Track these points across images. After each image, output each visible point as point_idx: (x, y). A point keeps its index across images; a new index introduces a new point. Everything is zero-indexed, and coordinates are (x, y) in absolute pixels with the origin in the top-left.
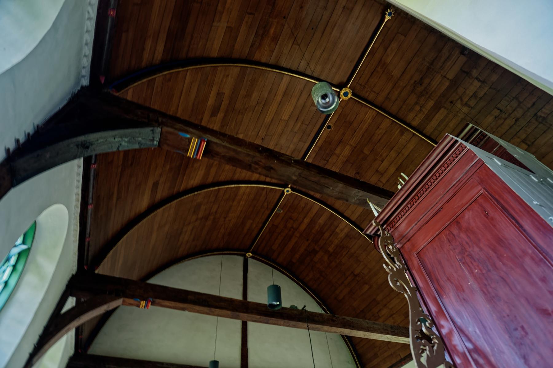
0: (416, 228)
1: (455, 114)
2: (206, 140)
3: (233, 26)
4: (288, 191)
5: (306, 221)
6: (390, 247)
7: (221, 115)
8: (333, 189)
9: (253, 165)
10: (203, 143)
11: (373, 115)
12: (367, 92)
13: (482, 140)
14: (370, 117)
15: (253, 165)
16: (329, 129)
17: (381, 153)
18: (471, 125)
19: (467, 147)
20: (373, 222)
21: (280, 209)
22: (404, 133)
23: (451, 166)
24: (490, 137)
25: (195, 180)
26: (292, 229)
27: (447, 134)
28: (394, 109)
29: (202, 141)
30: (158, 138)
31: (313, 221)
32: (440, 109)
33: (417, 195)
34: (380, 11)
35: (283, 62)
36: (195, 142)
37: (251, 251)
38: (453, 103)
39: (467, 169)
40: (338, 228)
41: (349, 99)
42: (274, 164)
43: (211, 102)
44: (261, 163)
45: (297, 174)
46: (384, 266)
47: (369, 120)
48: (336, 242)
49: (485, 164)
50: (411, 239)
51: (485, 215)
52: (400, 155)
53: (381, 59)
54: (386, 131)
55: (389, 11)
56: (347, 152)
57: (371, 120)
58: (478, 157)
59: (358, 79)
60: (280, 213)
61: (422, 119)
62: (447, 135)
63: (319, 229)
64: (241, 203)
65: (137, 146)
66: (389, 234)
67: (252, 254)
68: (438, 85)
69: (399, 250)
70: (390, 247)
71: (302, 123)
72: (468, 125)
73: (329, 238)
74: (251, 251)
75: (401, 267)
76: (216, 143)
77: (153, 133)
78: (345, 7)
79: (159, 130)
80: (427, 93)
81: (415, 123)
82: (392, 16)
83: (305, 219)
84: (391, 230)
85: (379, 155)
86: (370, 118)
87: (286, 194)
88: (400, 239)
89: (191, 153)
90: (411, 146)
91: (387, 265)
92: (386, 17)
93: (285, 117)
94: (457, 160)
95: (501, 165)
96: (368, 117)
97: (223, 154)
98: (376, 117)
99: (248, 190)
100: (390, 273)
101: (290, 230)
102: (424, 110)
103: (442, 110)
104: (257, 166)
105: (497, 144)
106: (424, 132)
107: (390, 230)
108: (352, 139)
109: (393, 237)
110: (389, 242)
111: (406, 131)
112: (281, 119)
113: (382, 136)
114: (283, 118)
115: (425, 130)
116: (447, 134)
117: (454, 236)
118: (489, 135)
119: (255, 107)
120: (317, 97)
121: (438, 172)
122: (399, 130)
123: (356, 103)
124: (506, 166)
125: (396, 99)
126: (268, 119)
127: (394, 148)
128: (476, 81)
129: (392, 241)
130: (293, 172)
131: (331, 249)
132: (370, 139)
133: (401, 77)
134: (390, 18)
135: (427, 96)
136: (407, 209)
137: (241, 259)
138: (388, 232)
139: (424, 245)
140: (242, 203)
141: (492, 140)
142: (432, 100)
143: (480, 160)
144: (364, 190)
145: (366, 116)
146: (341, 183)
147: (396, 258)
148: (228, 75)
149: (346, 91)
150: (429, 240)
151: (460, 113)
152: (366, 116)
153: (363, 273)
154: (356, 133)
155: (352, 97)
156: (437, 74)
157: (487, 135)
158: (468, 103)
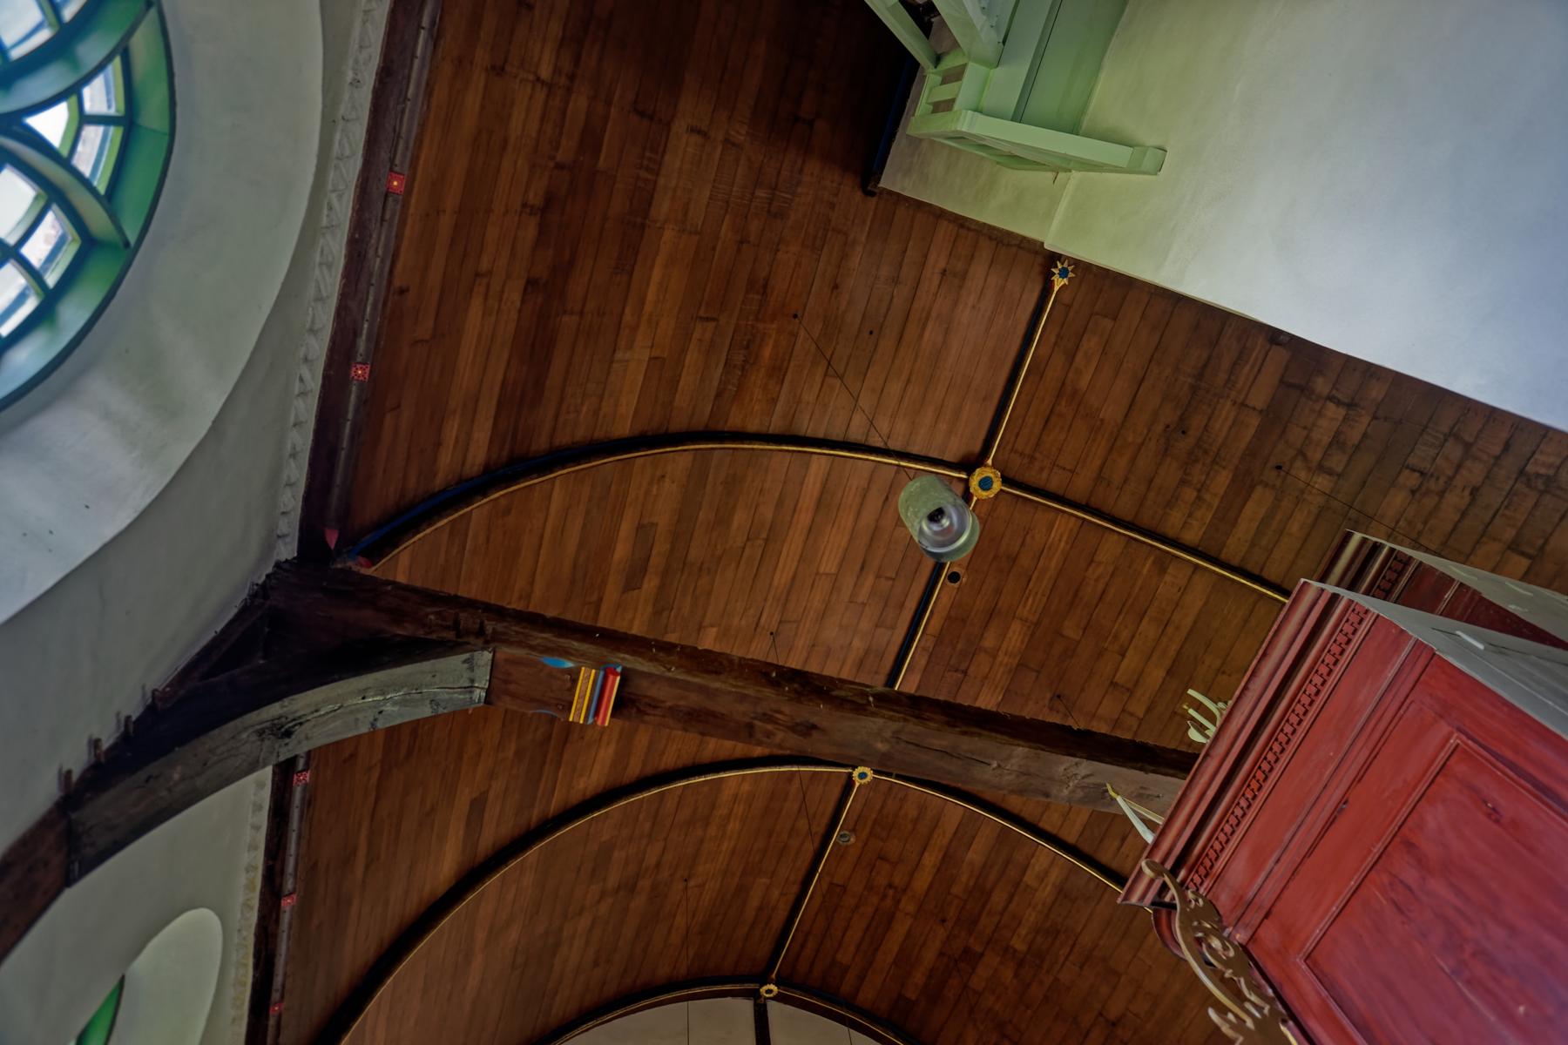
0: (1282, 870)
1: (1297, 497)
2: (619, 670)
3: (665, 356)
4: (862, 776)
5: (930, 860)
6: (1213, 945)
7: (650, 584)
8: (999, 766)
9: (758, 723)
10: (611, 677)
11: (1071, 530)
12: (1042, 470)
13: (1400, 574)
14: (1062, 536)
15: (758, 723)
16: (955, 582)
17: (1114, 631)
18: (1357, 537)
19: (1371, 609)
20: (1143, 864)
21: (847, 833)
22: (1168, 568)
23: (1338, 671)
24: (1421, 563)
25: (589, 776)
26: (891, 892)
27: (1303, 580)
28: (1124, 508)
29: (609, 672)
30: (484, 682)
31: (949, 859)
32: (1252, 488)
33: (1260, 767)
34: (1037, 269)
35: (806, 422)
36: (588, 678)
37: (774, 976)
38: (1285, 468)
39: (1390, 674)
40: (1028, 872)
41: (997, 495)
42: (818, 713)
43: (621, 551)
44: (778, 716)
45: (888, 734)
46: (1212, 1014)
47: (1062, 544)
48: (1031, 917)
49: (1440, 657)
50: (1275, 910)
51: (1489, 816)
52: (1170, 630)
53: (1063, 384)
54: (1116, 569)
55: (1060, 266)
57: (1067, 543)
58: (1411, 636)
59: (1013, 439)
60: (849, 843)
61: (1208, 522)
62: (1305, 583)
63: (971, 883)
64: (730, 826)
65: (426, 711)
66: (1201, 896)
67: (778, 988)
68: (1230, 428)
69: (1244, 948)
70: (1216, 943)
71: (878, 577)
72: (1347, 537)
73: (1006, 907)
74: (774, 976)
75: (1266, 1011)
76: (649, 675)
77: (471, 669)
78: (945, 271)
79: (487, 656)
80: (1206, 452)
81: (1191, 536)
82: (1069, 276)
83: (926, 854)
84: (1205, 885)
85: (1110, 638)
86: (1064, 538)
87: (857, 784)
88: (1239, 913)
89: (578, 713)
90: (1195, 601)
91: (1222, 1010)
92: (1056, 280)
93: (829, 565)
94: (1350, 650)
95: (1485, 649)
96: (1057, 539)
97: (669, 704)
98: (1078, 533)
99: (746, 787)
100: (1237, 1039)
101: (884, 897)
102: (1207, 497)
103: (1259, 490)
104: (769, 727)
105: (1447, 581)
106: (1223, 557)
107: (1201, 884)
108: (1022, 603)
109: (1214, 906)
110: (1208, 926)
111: (1170, 562)
112: (817, 573)
113: (1107, 585)
114: (821, 571)
115: (1225, 550)
116: (1303, 580)
117: (1409, 888)
118: (1419, 556)
119: (744, 548)
120: (917, 521)
121: (1305, 692)
122: (1152, 558)
123: (1017, 503)
124: (1500, 650)
125: (1126, 480)
126: (782, 578)
127: (1148, 613)
128: (1331, 406)
129: (1214, 922)
130: (876, 730)
132: (1076, 595)
133: (1124, 421)
134: (1065, 281)
136: (1239, 812)
137: (746, 1007)
138: (1196, 892)
139: (1321, 926)
140: (733, 826)
141: (1431, 570)
142: (1224, 468)
143: (1419, 645)
144: (1090, 757)
145: (1050, 533)
146: (1019, 745)
147: (1242, 980)
148: (663, 477)
149: (985, 475)
150: (1334, 908)
151: (1310, 493)
152: (1053, 535)
153: (1135, 1015)
154: (1032, 583)
155: (1003, 488)
156: (1221, 401)
157: (1410, 558)
158: (1327, 464)
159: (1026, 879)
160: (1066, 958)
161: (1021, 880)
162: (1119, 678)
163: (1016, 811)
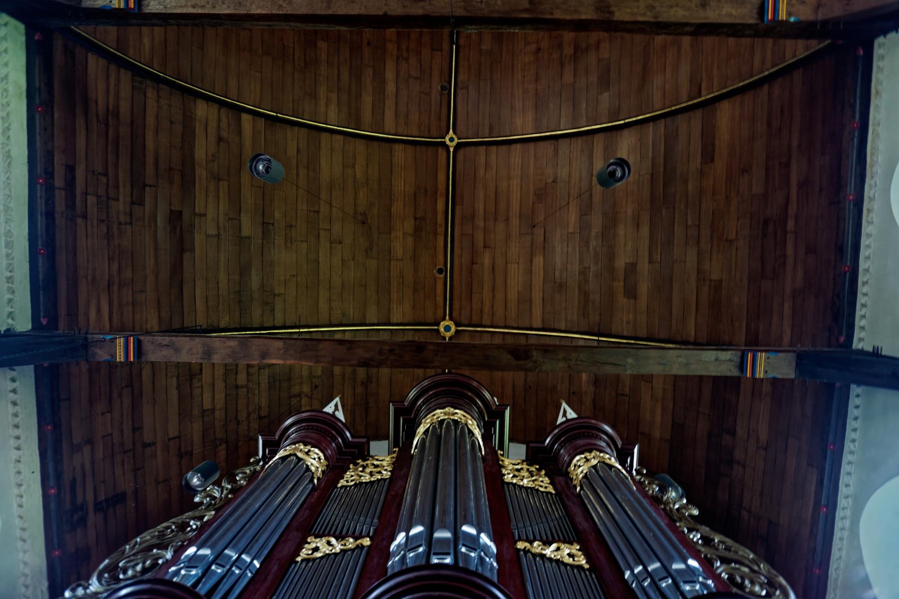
4: (451, 140)
5: (391, 88)
56: (397, 247)
57: (393, 308)
63: (363, 79)
90: (323, 305)
96: (398, 310)
101: (408, 50)
112: (518, 263)
131: (322, 45)
135: (347, 376)
159: (336, 95)
160: (294, 48)
161: (338, 93)
162: (339, 246)
163: (357, 139)
